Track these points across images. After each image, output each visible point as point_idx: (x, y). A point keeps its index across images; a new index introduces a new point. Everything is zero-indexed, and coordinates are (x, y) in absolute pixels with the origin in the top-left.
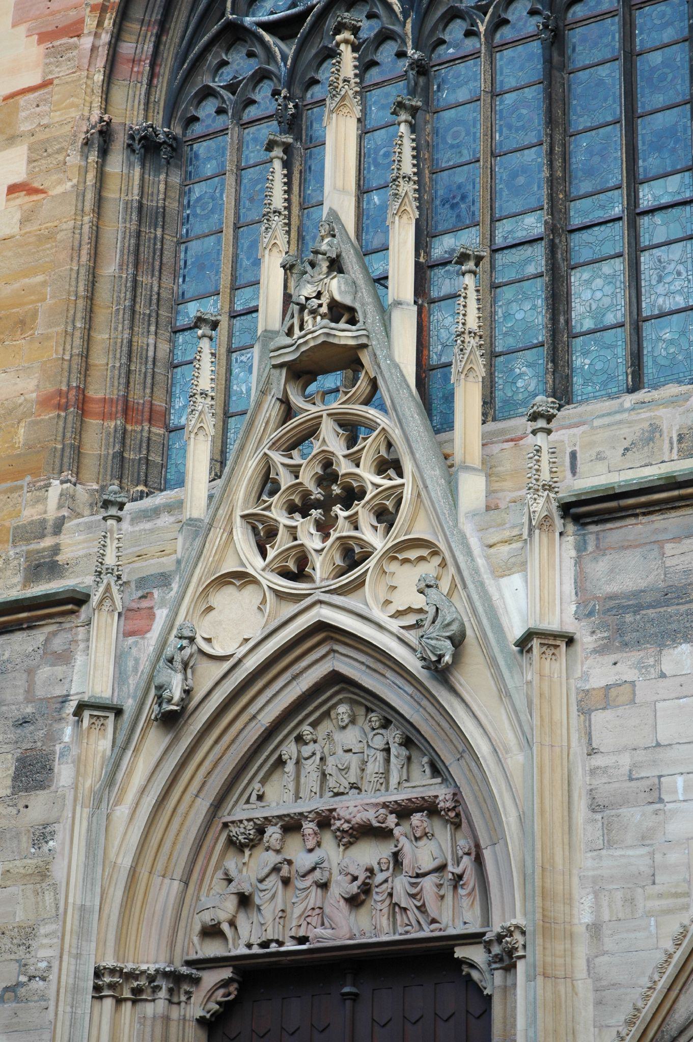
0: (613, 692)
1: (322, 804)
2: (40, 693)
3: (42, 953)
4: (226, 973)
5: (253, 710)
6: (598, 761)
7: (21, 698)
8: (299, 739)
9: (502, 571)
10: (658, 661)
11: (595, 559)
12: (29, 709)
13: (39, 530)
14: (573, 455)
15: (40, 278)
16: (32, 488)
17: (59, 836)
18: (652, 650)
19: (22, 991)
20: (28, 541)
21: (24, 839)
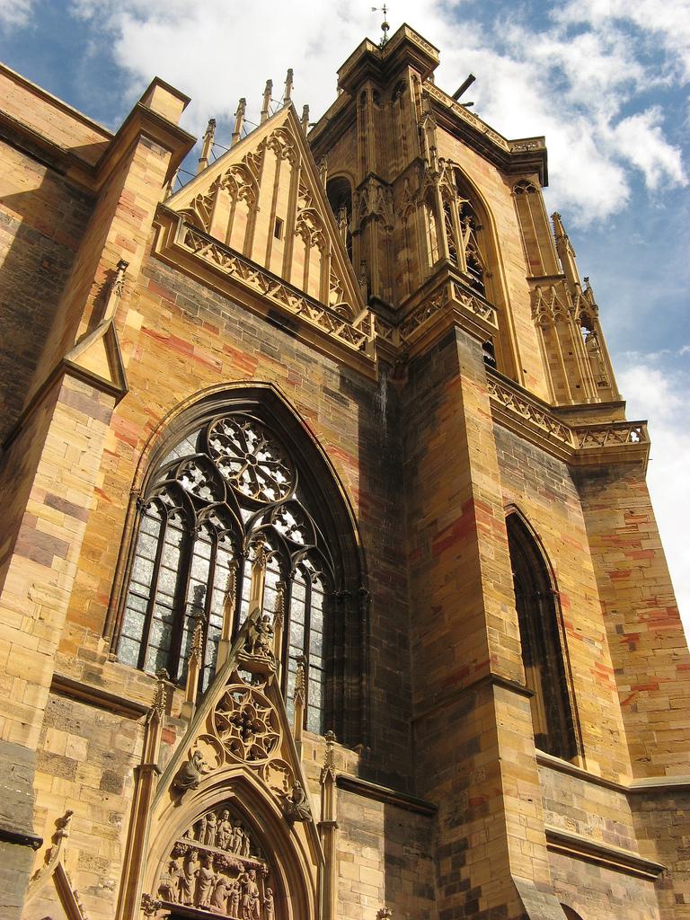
0: (348, 855)
1: (218, 851)
2: (118, 746)
3: (111, 876)
4: (169, 912)
5: (203, 798)
6: (341, 880)
7: (107, 743)
8: (209, 818)
9: (313, 791)
10: (361, 851)
11: (343, 802)
12: (111, 751)
13: (92, 656)
14: (315, 752)
15: (105, 539)
16: (90, 634)
17: (123, 821)
18: (359, 845)
19: (100, 892)
20: (87, 659)
21: (105, 815)
